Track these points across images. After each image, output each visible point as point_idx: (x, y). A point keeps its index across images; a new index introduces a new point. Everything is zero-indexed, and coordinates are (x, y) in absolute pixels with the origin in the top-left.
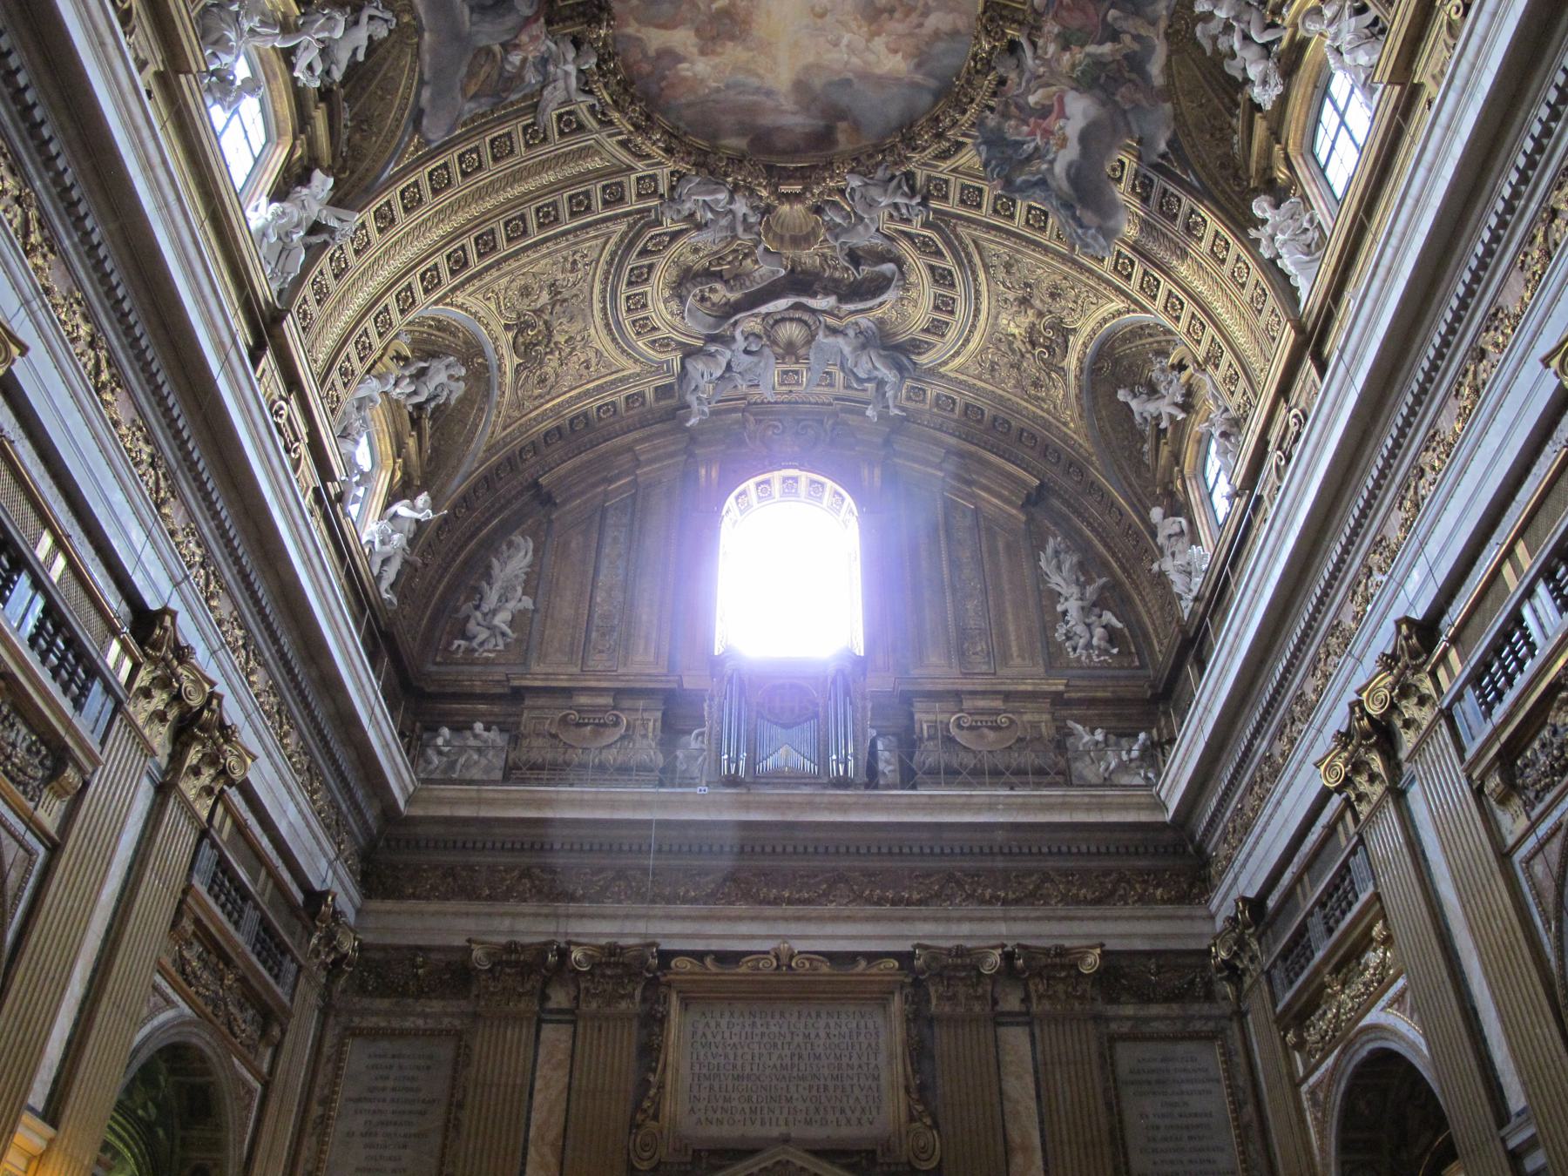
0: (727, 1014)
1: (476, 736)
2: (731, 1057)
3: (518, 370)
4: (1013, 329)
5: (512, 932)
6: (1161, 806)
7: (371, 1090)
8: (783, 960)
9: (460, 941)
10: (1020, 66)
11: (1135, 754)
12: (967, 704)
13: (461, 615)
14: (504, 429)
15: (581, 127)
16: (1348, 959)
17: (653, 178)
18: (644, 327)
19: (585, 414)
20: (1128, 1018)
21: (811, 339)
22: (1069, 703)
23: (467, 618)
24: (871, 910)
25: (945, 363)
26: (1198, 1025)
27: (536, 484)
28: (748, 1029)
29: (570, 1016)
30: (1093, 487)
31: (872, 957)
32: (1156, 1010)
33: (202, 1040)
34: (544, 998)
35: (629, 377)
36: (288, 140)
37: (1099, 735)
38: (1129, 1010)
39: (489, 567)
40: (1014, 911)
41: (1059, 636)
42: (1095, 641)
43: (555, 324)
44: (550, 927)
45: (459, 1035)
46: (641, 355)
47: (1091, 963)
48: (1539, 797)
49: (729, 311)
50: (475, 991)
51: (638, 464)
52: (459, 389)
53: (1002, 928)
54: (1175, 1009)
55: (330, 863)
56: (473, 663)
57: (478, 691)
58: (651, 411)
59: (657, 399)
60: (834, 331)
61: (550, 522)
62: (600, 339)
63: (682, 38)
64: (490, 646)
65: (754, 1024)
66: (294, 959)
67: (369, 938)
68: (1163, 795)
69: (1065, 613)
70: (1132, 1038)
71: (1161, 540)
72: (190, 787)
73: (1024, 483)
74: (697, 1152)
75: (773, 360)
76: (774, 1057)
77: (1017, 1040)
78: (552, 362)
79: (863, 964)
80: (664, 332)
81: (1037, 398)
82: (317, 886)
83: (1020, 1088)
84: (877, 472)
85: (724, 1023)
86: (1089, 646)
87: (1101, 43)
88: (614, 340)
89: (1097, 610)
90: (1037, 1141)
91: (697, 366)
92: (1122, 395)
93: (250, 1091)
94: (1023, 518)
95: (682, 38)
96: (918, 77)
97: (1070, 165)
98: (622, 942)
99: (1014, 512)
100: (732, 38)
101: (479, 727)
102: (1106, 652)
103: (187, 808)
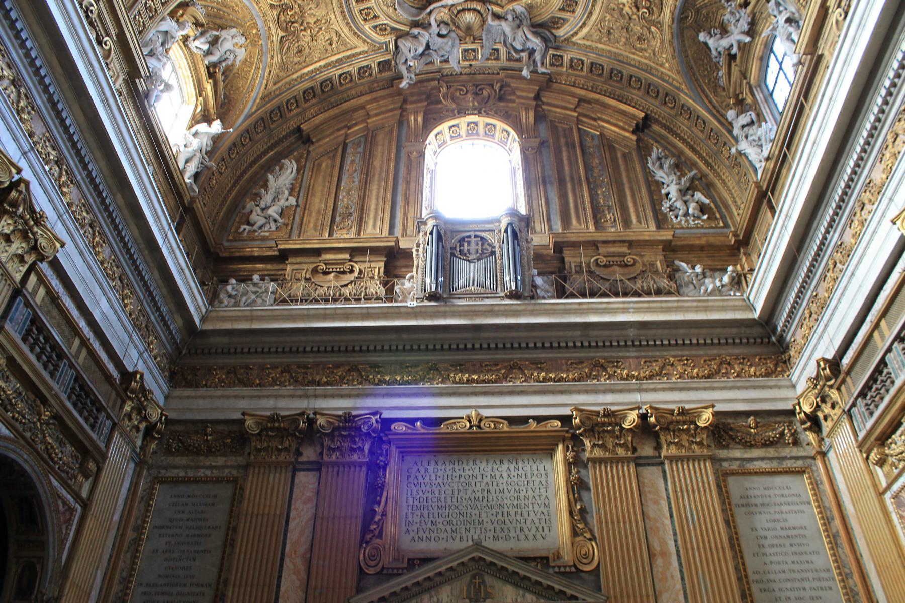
0: (433, 463)
2: (437, 493)
3: (282, 40)
6: (752, 308)
7: (171, 520)
9: (237, 415)
12: (603, 250)
13: (247, 210)
14: (274, 84)
18: (368, 15)
19: (330, 79)
20: (736, 459)
25: (576, 33)
26: (789, 464)
27: (299, 129)
28: (450, 473)
29: (317, 467)
30: (684, 109)
31: (540, 419)
34: (299, 454)
35: (360, 54)
38: (737, 453)
40: (646, 384)
42: (691, 211)
43: (307, 8)
45: (235, 481)
46: (368, 37)
50: (247, 451)
51: (368, 116)
52: (242, 54)
54: (771, 452)
55: (141, 355)
57: (256, 254)
58: (376, 81)
59: (380, 71)
60: (497, 16)
61: (309, 152)
62: (338, 23)
64: (267, 228)
65: (453, 470)
66: (108, 417)
67: (172, 415)
68: (751, 298)
71: (736, 131)
73: (633, 116)
75: (457, 41)
76: (469, 492)
78: (306, 38)
80: (383, 20)
81: (641, 50)
82: (130, 369)
85: (431, 469)
86: (686, 214)
88: (348, 24)
91: (404, 45)
93: (72, 510)
99: (627, 134)
102: (699, 218)
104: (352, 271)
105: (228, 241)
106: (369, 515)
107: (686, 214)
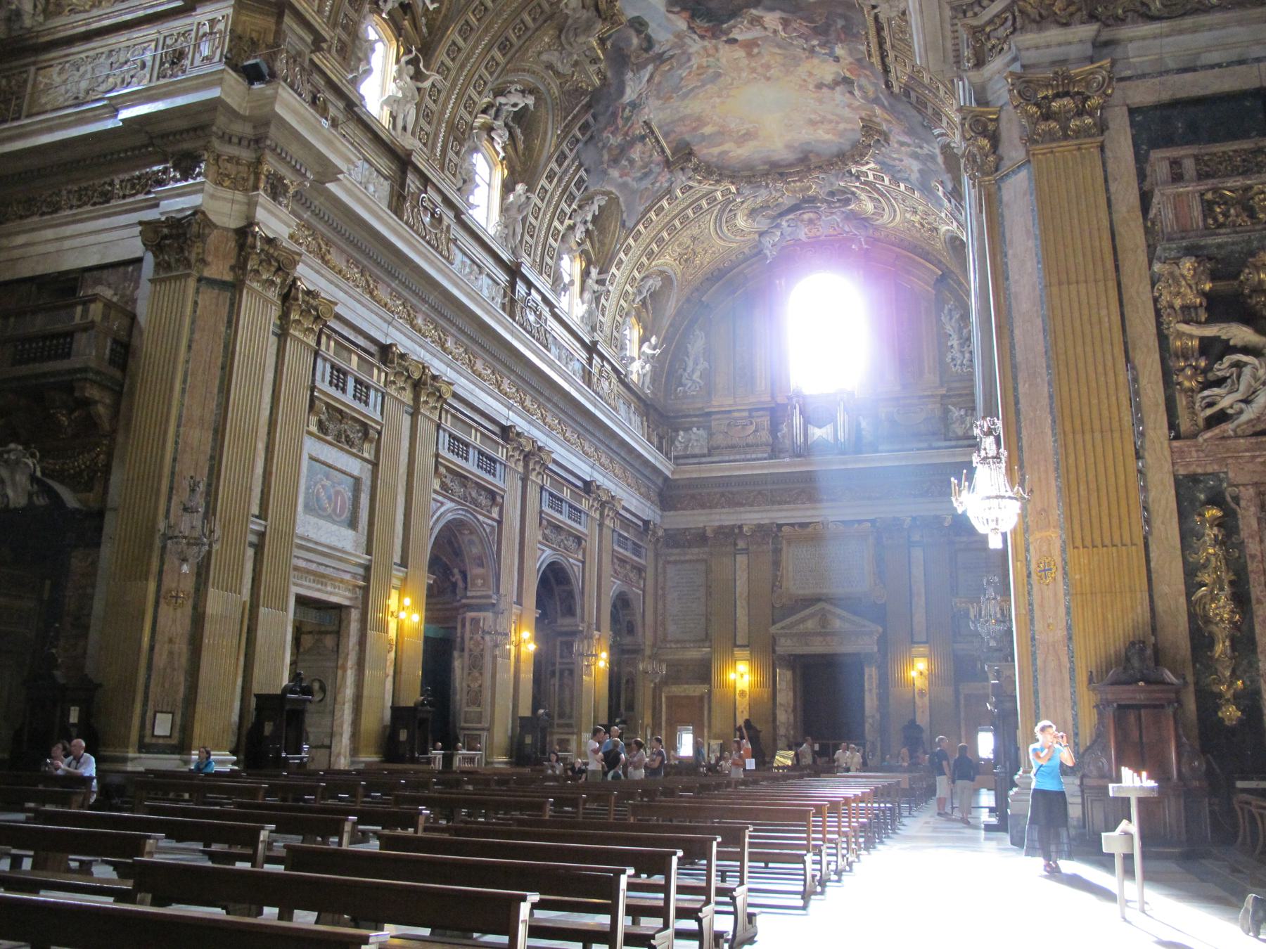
9: (701, 525)
15: (691, 187)
21: (819, 219)
22: (949, 397)
23: (681, 376)
29: (746, 551)
31: (860, 522)
33: (625, 588)
34: (735, 544)
36: (578, 260)
39: (686, 348)
41: (948, 360)
45: (706, 561)
49: (774, 218)
63: (726, 147)
64: (693, 388)
67: (666, 527)
69: (952, 346)
72: (607, 522)
73: (935, 273)
79: (856, 525)
86: (962, 365)
90: (923, 590)
93: (639, 595)
94: (934, 292)
95: (726, 147)
96: (841, 141)
103: (608, 527)
104: (751, 423)
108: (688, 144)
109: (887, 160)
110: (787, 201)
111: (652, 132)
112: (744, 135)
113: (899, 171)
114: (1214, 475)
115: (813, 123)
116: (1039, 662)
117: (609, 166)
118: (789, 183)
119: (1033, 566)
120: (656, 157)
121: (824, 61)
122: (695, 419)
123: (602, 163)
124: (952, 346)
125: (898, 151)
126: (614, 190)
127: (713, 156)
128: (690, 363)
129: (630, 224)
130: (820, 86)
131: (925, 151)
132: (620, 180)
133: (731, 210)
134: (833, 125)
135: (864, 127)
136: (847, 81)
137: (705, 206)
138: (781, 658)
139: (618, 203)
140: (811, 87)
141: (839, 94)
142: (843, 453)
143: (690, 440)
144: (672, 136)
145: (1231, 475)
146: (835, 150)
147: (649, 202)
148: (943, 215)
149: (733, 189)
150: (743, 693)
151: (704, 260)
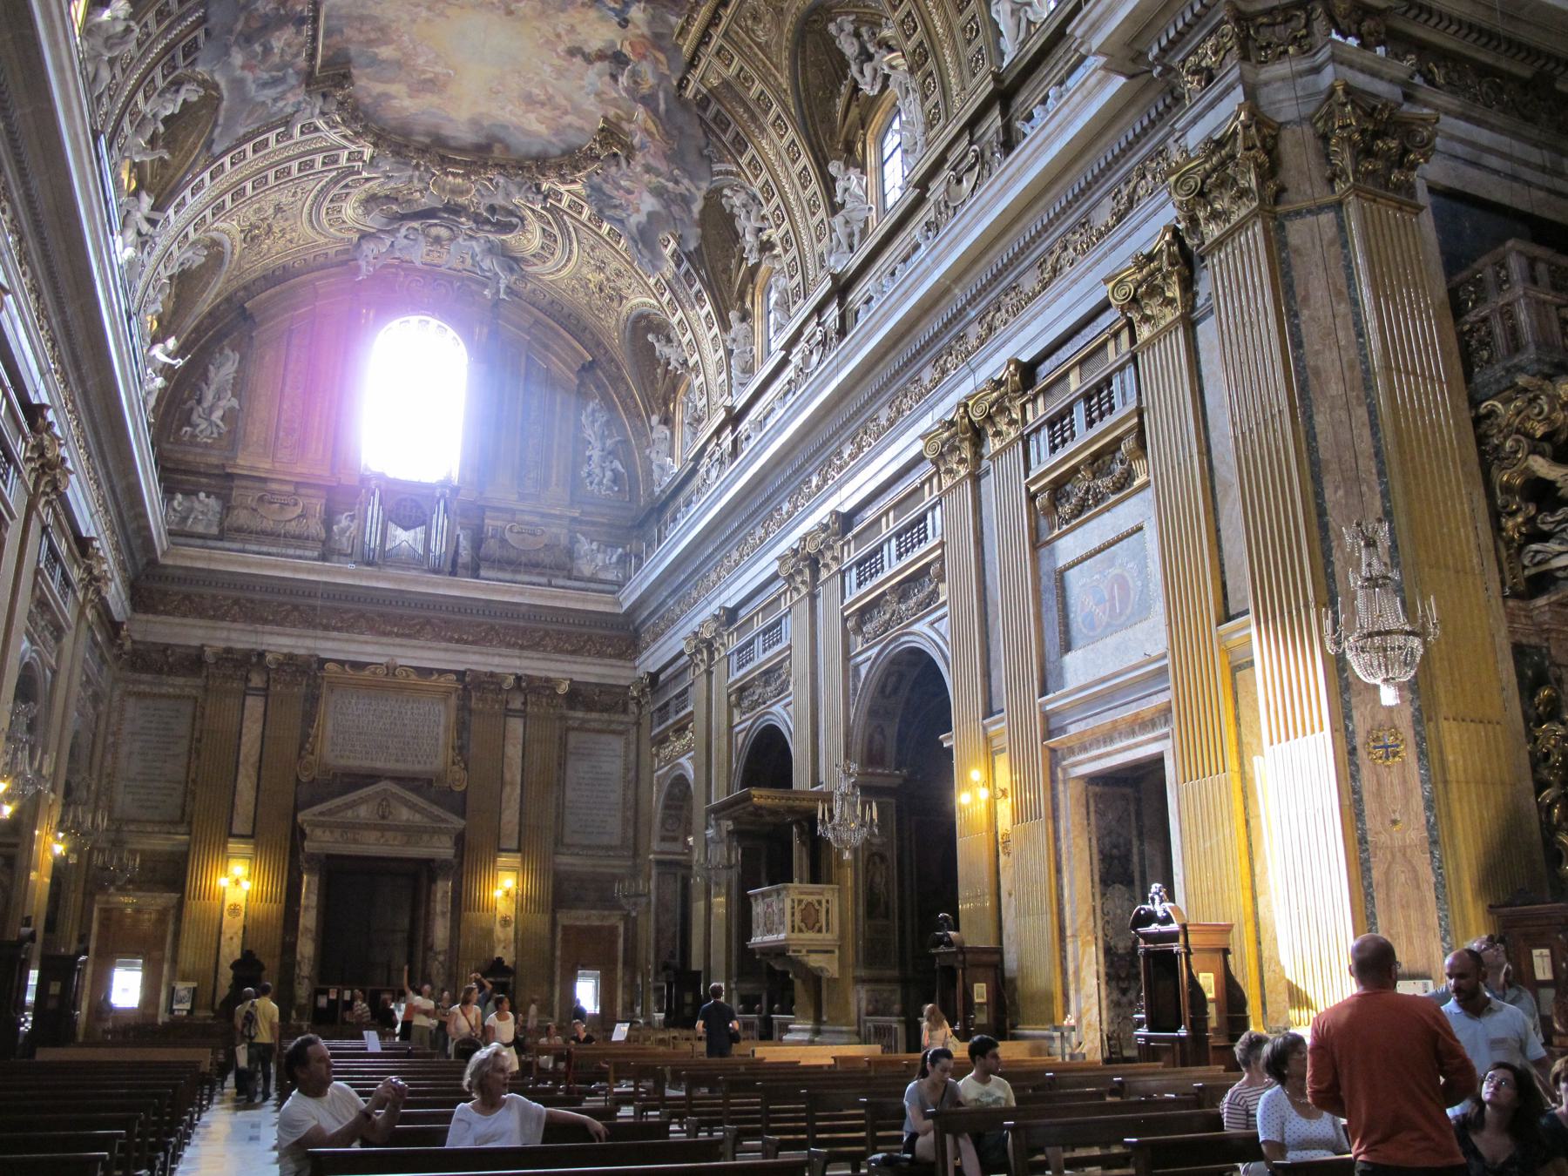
1: (200, 502)
4: (590, 276)
5: (228, 639)
7: (143, 728)
8: (391, 670)
9: (196, 643)
10: (618, 165)
11: (614, 559)
15: (317, 129)
16: (681, 729)
17: (361, 153)
20: (578, 719)
22: (580, 522)
23: (191, 410)
24: (444, 645)
26: (614, 726)
27: (242, 306)
31: (442, 672)
32: (594, 715)
34: (247, 680)
37: (595, 546)
38: (580, 714)
39: (206, 370)
40: (526, 653)
41: (583, 474)
44: (253, 638)
47: (563, 689)
48: (744, 714)
50: (204, 673)
53: (517, 662)
54: (606, 716)
56: (198, 445)
63: (393, 89)
70: (579, 729)
73: (582, 357)
74: (335, 775)
77: (516, 726)
79: (435, 677)
80: (350, 223)
83: (514, 752)
84: (485, 330)
86: (600, 483)
87: (668, 180)
88: (313, 227)
89: (611, 457)
92: (650, 337)
95: (393, 89)
96: (554, 140)
97: (639, 223)
98: (296, 652)
99: (571, 376)
100: (432, 92)
101: (202, 495)
105: (168, 442)
106: (305, 736)
107: (600, 483)
108: (348, 61)
109: (607, 188)
110: (425, 202)
111: (315, 20)
112: (426, 81)
113: (615, 207)
114: (1538, 648)
115: (530, 101)
116: (1376, 874)
117: (236, 42)
118: (447, 174)
119: (1359, 740)
120: (302, 62)
121: (603, 19)
122: (204, 480)
123: (230, 32)
124: (590, 458)
125: (634, 179)
126: (223, 84)
127: (369, 95)
128: (209, 396)
129: (217, 149)
130: (573, 52)
131: (681, 189)
132: (238, 73)
133: (346, 186)
134: (558, 113)
135: (602, 130)
136: (619, 59)
137: (318, 166)
138: (312, 857)
139: (216, 109)
140: (561, 48)
141: (595, 76)
142: (436, 571)
143: (191, 510)
144: (337, 38)
145: (1553, 652)
146: (535, 149)
147: (254, 126)
148: (652, 281)
149: (368, 152)
150: (235, 910)
151: (274, 252)
